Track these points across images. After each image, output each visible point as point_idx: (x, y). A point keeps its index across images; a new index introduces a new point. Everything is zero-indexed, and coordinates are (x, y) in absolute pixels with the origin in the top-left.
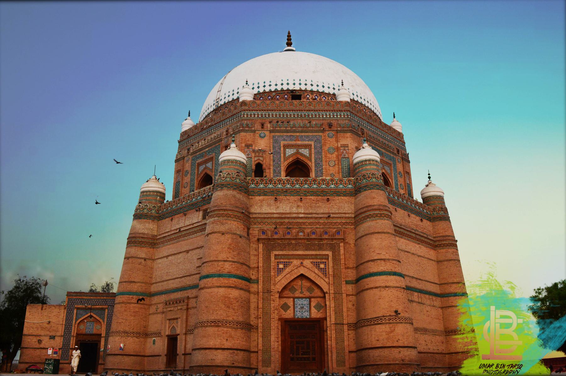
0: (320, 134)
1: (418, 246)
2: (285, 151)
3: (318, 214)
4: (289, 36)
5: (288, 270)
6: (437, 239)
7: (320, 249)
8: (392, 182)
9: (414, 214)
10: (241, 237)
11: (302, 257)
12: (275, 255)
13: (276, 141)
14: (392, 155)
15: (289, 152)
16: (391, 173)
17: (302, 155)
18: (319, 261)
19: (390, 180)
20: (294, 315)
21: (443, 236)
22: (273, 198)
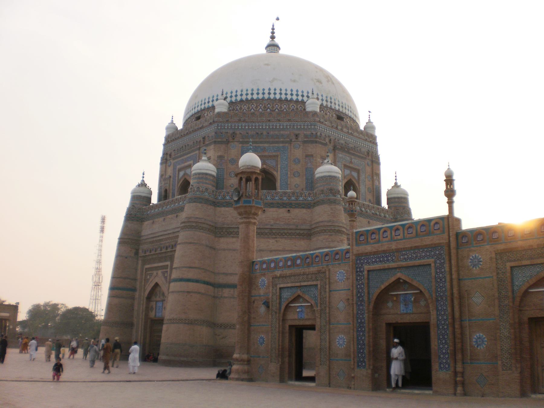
0: (197, 152)
1: (271, 241)
2: (179, 173)
3: (169, 230)
4: (273, 29)
5: (151, 280)
6: (313, 226)
7: (166, 261)
8: (278, 175)
9: (273, 207)
10: (126, 258)
11: (157, 268)
12: (146, 269)
13: (174, 169)
14: (281, 145)
15: (182, 173)
16: (277, 165)
17: (187, 174)
18: (165, 270)
19: (275, 173)
20: (155, 315)
21: (317, 223)
22: (151, 221)
